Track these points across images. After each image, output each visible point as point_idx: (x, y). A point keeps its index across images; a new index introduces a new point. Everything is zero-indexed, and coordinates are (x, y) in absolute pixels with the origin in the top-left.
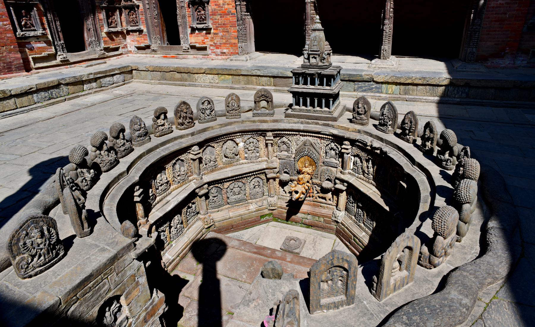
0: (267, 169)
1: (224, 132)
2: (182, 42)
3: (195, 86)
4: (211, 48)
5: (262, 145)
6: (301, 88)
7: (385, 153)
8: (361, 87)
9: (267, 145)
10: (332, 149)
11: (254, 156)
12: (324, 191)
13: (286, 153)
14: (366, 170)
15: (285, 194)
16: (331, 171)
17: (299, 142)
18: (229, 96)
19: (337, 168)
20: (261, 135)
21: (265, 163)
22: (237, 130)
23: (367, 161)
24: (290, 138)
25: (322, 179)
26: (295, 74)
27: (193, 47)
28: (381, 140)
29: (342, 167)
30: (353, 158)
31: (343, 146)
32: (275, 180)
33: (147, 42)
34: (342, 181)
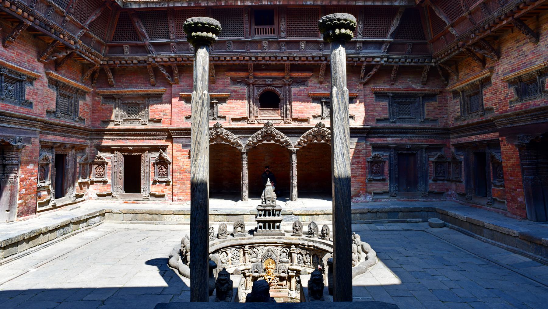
0: (245, 270)
1: (223, 246)
2: (142, 191)
3: (164, 224)
4: (169, 195)
5: (241, 254)
6: (263, 218)
7: (317, 247)
8: (286, 219)
10: (284, 252)
14: (306, 260)
18: (222, 224)
20: (241, 248)
22: (229, 244)
23: (306, 255)
24: (258, 248)
26: (259, 210)
27: (152, 195)
28: (313, 241)
29: (292, 262)
33: (109, 191)
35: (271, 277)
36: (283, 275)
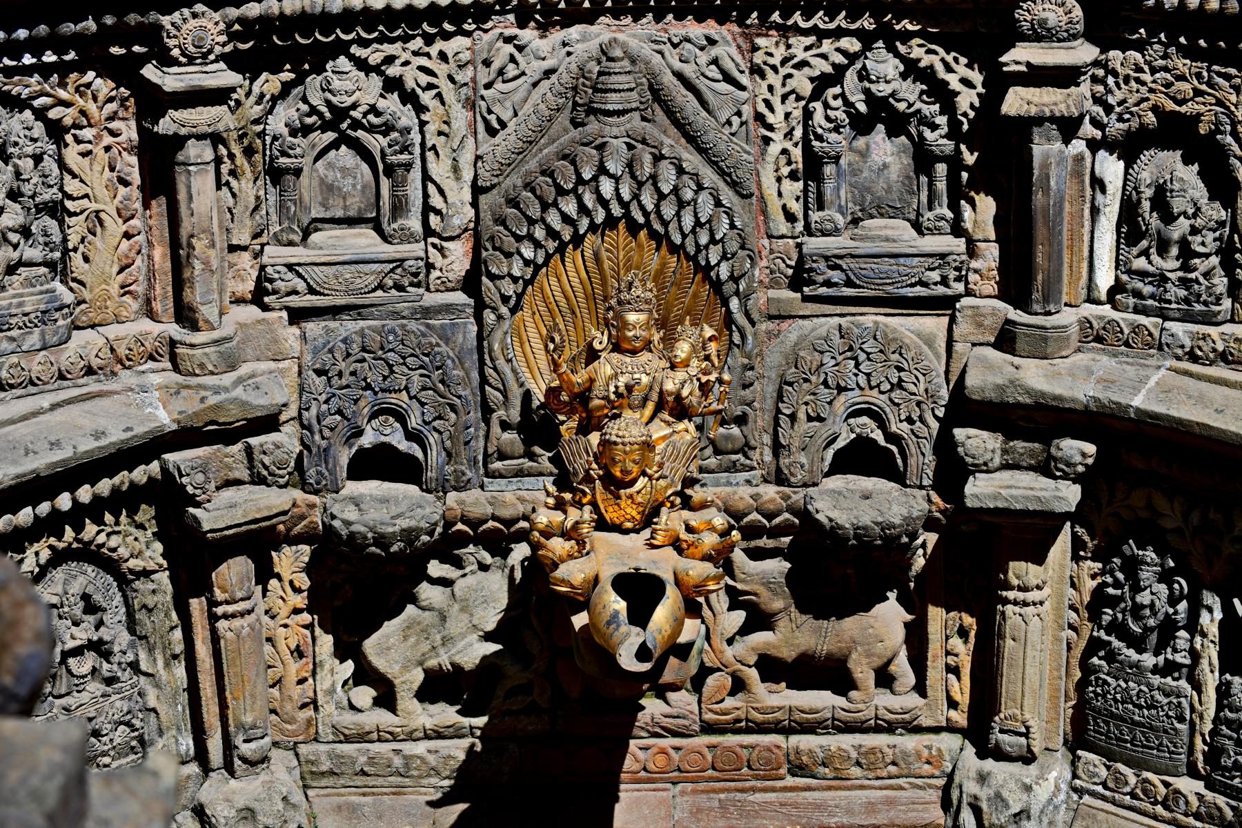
0: (186, 437)
5: (101, 172)
9: (159, 167)
10: (881, 114)
11: (32, 303)
12: (834, 571)
13: (364, 241)
15: (383, 718)
16: (891, 346)
17: (503, 100)
19: (946, 304)
20: (92, 55)
21: (159, 376)
24: (408, 59)
25: (799, 462)
29: (1017, 282)
30: (1111, 168)
31: (1019, 56)
32: (265, 573)
34: (1033, 424)
35: (664, 564)
36: (852, 504)
